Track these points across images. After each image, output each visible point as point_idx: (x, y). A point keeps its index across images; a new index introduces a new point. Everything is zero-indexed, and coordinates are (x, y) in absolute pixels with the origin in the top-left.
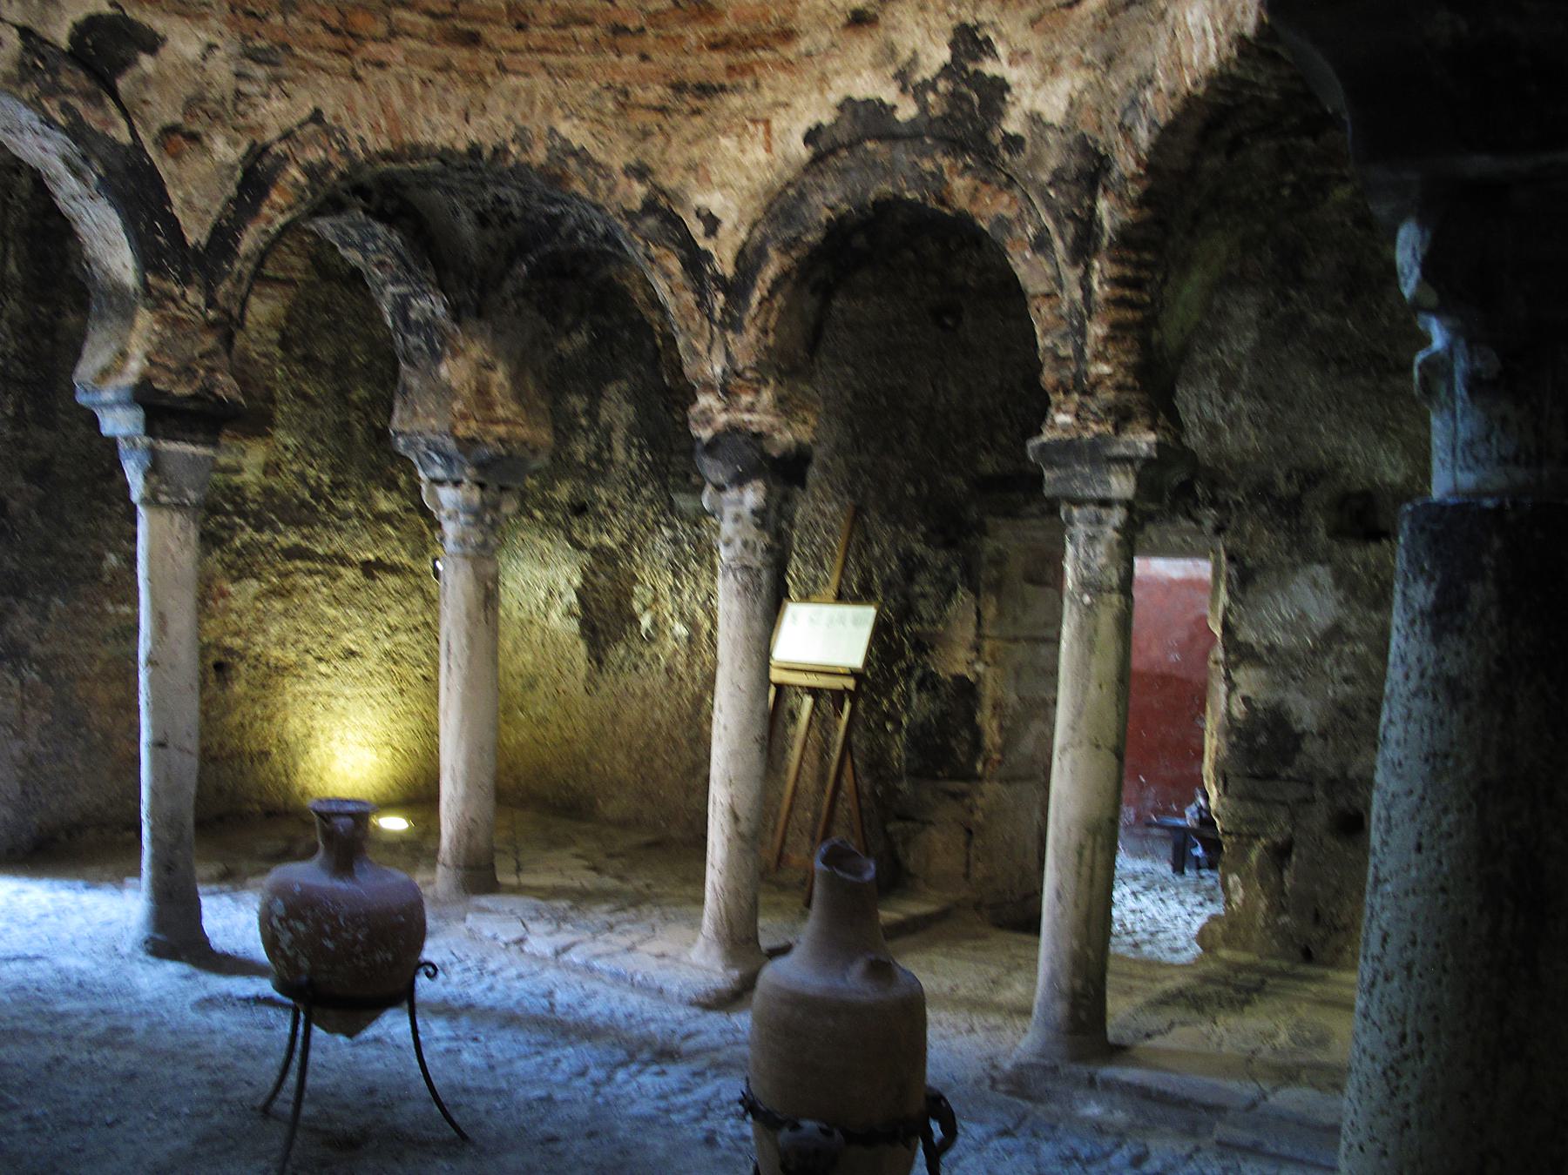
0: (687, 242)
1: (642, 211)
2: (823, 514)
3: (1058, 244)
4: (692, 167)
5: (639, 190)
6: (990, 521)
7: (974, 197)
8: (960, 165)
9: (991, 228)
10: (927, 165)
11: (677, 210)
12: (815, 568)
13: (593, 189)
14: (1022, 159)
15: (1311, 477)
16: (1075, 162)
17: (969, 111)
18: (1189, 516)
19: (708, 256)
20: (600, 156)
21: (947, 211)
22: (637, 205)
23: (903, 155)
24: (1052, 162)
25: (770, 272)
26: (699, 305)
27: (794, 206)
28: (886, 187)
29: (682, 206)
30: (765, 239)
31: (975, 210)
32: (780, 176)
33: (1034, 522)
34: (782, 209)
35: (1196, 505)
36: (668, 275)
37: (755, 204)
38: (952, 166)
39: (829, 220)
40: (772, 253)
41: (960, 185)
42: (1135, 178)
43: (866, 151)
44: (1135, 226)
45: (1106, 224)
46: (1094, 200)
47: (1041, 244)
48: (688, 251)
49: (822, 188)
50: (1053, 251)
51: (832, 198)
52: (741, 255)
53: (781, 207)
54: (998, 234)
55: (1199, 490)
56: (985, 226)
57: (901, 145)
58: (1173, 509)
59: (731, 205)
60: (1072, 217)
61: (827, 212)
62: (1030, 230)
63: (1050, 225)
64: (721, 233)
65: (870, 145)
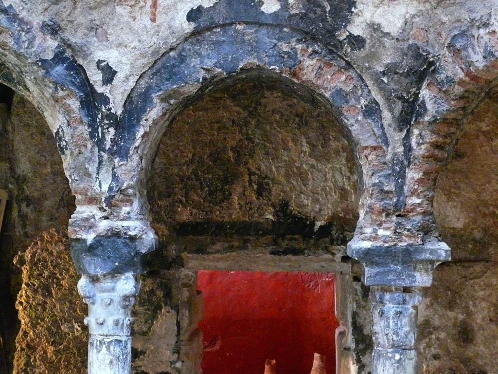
0: (86, 86)
1: (53, 59)
2: (51, 253)
3: (386, 114)
4: (93, 28)
5: (52, 44)
6: (184, 255)
7: (319, 76)
8: (310, 50)
9: (332, 96)
10: (285, 48)
11: (80, 61)
12: (43, 295)
13: (18, 41)
14: (362, 53)
16: (407, 63)
18: (327, 250)
19: (105, 100)
20: (23, 14)
21: (295, 80)
22: (50, 56)
23: (265, 37)
24: (388, 59)
25: (154, 113)
26: (92, 135)
27: (174, 66)
28: (253, 60)
29: (85, 57)
30: (149, 88)
31: (319, 82)
32: (165, 43)
33: (217, 255)
34: (164, 67)
35: (332, 244)
36: (68, 111)
37: (145, 61)
39: (205, 79)
40: (156, 100)
41: (309, 66)
42: (461, 83)
43: (236, 31)
44: (453, 111)
45: (429, 106)
46: (419, 89)
47: (372, 111)
48: (84, 92)
49: (200, 55)
50: (381, 118)
51: (209, 64)
52: (129, 99)
53: (164, 65)
54: (338, 102)
55: (333, 232)
56: (327, 95)
57: (264, 31)
58: (317, 247)
59: (124, 60)
60: (401, 98)
61: (203, 72)
62: (363, 102)
64: (115, 82)
65: (239, 27)
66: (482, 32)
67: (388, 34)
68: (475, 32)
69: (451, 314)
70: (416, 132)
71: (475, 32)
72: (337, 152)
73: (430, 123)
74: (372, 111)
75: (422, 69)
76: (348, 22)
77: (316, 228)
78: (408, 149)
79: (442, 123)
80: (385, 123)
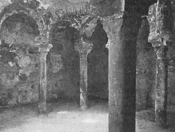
3: (44, 23)
15: (26, 46)
17: (34, 5)
24: (45, 14)
38: (31, 10)
47: (41, 22)
50: (43, 23)
63: (42, 19)
66: (61, 11)
67: (45, 9)
68: (60, 11)
69: (34, 62)
70: (49, 26)
71: (60, 11)
72: (13, 32)
73: (51, 25)
74: (41, 22)
75: (49, 15)
76: (39, 6)
77: (10, 46)
78: (47, 29)
79: (53, 25)
80: (44, 24)
